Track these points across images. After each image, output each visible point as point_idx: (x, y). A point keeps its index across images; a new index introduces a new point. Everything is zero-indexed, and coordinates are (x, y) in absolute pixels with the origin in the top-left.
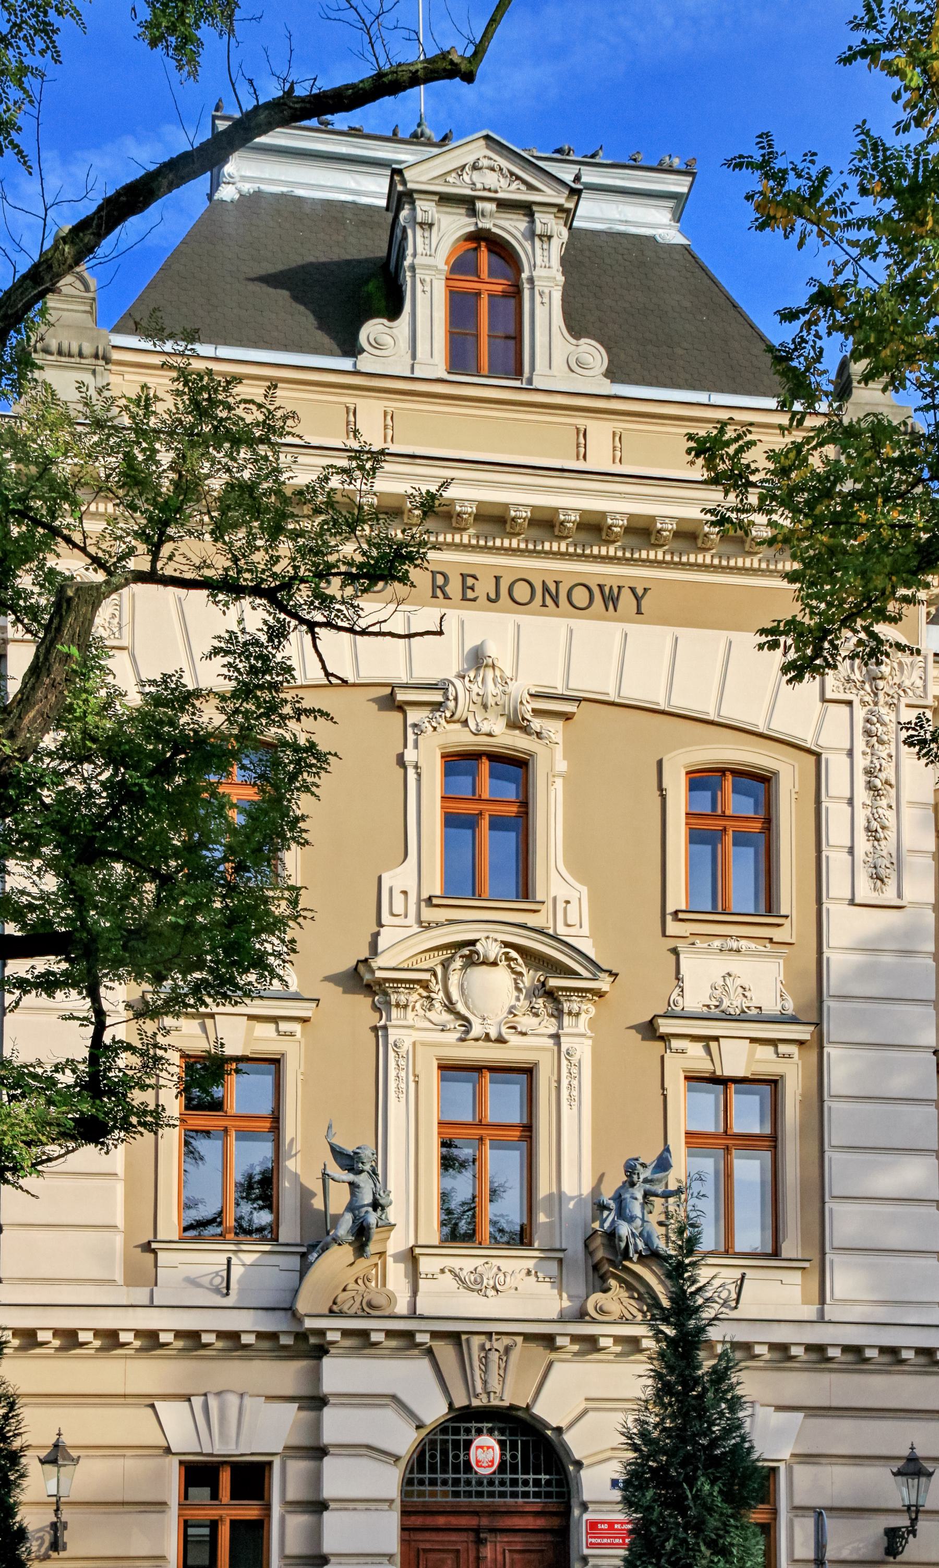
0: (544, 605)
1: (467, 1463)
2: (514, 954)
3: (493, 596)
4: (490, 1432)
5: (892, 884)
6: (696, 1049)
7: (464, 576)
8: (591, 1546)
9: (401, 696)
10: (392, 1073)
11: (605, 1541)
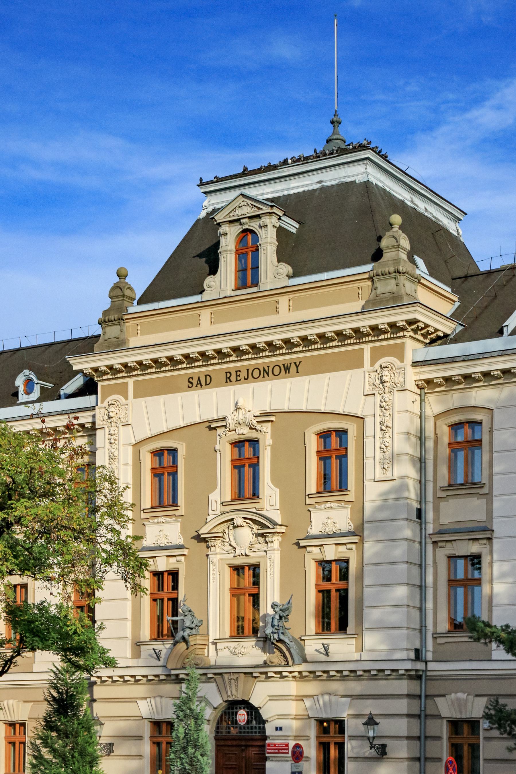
0: (264, 377)
1: (236, 720)
2: (248, 521)
3: (246, 378)
4: (244, 708)
5: (390, 470)
6: (316, 550)
7: (236, 372)
8: (269, 753)
9: (213, 425)
10: (211, 572)
11: (273, 751)
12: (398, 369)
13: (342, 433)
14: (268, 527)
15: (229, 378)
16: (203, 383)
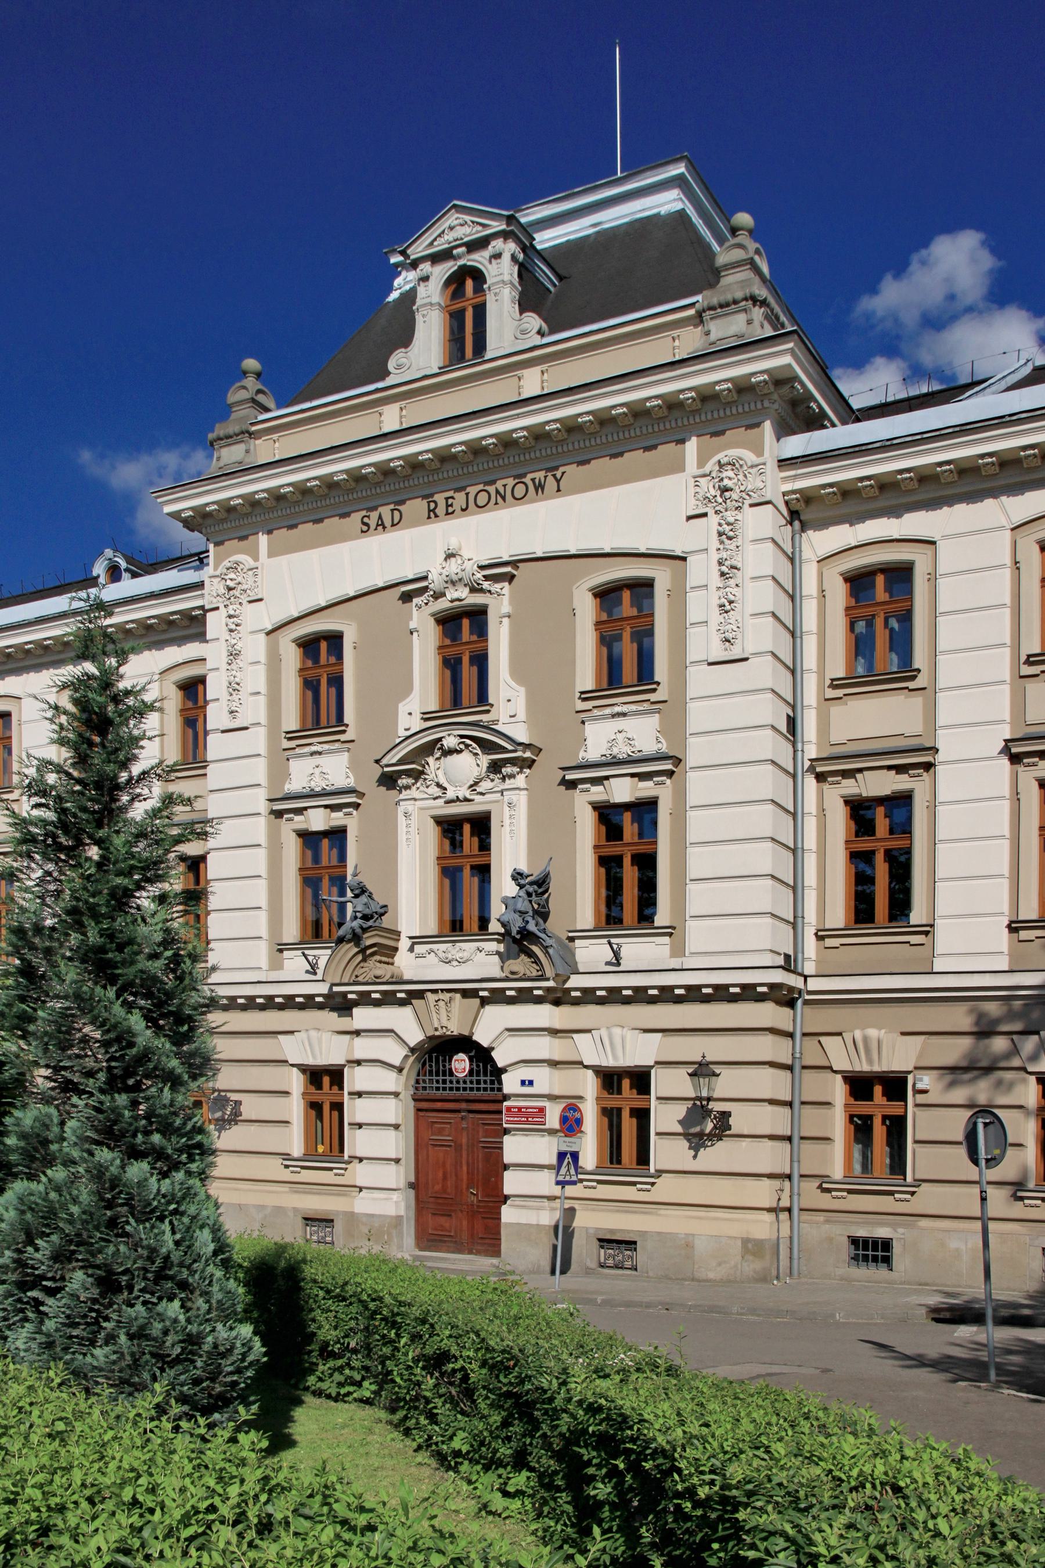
1: (450, 1070)
2: (468, 742)
8: (508, 1122)
12: (752, 467)
13: (643, 587)
14: (505, 750)
15: (433, 511)
16: (388, 522)
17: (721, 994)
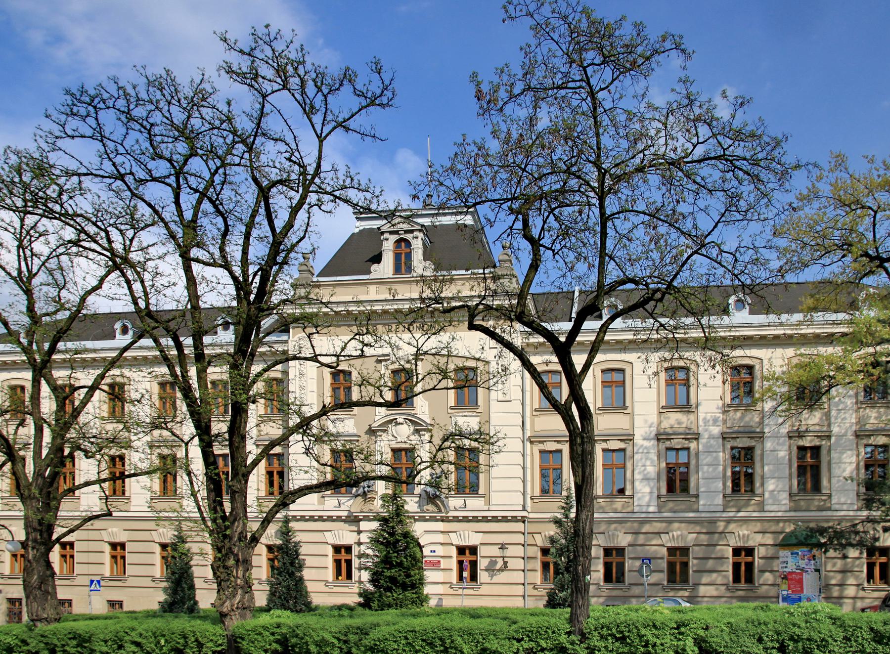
17: (505, 519)
